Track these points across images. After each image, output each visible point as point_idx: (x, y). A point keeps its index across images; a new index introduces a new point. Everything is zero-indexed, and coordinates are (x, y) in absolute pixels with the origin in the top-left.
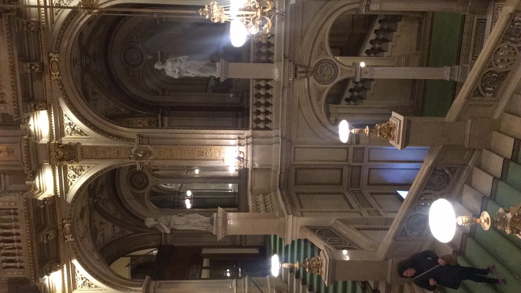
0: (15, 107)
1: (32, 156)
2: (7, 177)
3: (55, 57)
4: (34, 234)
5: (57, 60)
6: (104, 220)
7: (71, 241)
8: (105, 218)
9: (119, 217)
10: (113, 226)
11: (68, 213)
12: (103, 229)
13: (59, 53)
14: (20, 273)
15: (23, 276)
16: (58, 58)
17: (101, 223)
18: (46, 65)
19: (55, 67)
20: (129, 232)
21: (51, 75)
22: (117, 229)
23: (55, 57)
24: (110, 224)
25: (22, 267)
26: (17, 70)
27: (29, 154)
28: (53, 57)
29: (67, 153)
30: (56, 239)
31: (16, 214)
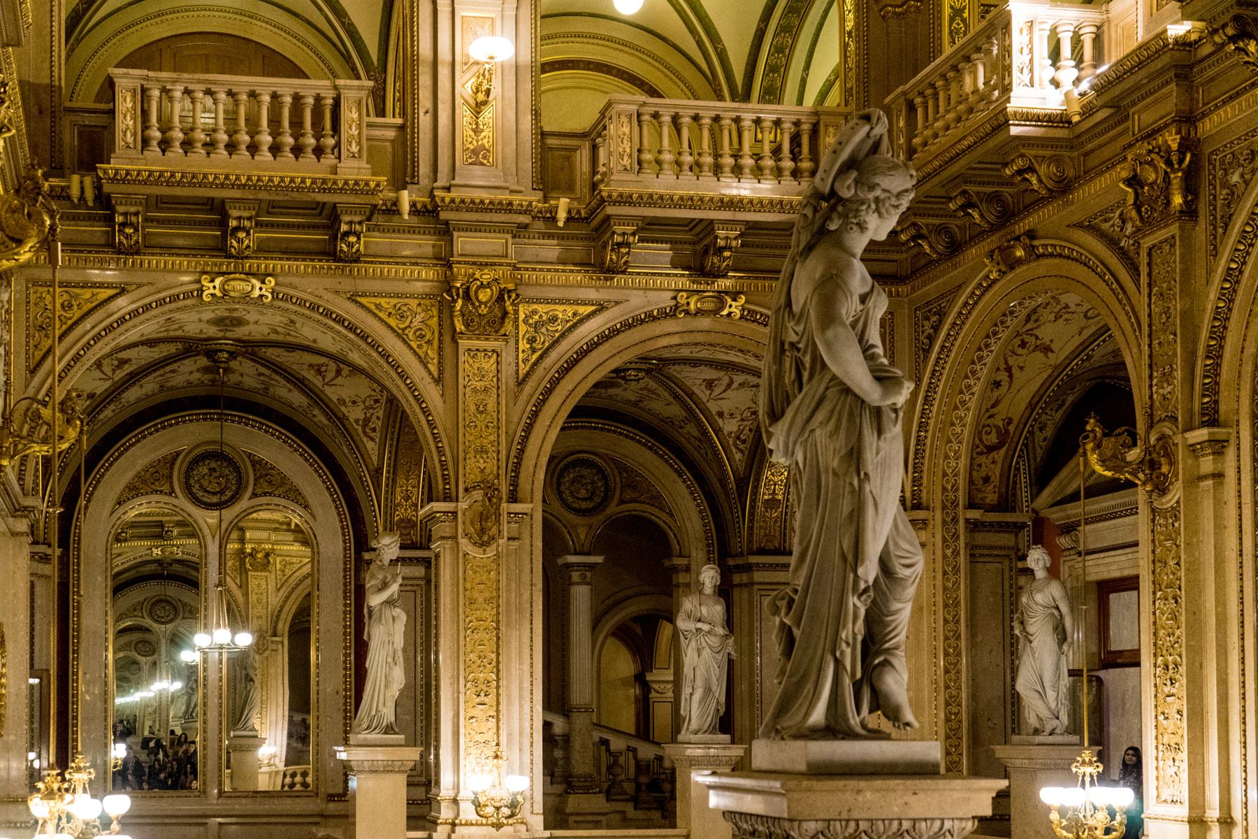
0: (635, 196)
1: (487, 217)
2: (391, 134)
3: (734, 308)
5: (725, 312)
6: (120, 374)
7: (201, 291)
11: (292, 292)
13: (741, 318)
15: (119, 143)
16: (729, 314)
18: (713, 283)
19: (709, 306)
21: (691, 292)
23: (734, 308)
24: (101, 387)
27: (487, 210)
28: (734, 304)
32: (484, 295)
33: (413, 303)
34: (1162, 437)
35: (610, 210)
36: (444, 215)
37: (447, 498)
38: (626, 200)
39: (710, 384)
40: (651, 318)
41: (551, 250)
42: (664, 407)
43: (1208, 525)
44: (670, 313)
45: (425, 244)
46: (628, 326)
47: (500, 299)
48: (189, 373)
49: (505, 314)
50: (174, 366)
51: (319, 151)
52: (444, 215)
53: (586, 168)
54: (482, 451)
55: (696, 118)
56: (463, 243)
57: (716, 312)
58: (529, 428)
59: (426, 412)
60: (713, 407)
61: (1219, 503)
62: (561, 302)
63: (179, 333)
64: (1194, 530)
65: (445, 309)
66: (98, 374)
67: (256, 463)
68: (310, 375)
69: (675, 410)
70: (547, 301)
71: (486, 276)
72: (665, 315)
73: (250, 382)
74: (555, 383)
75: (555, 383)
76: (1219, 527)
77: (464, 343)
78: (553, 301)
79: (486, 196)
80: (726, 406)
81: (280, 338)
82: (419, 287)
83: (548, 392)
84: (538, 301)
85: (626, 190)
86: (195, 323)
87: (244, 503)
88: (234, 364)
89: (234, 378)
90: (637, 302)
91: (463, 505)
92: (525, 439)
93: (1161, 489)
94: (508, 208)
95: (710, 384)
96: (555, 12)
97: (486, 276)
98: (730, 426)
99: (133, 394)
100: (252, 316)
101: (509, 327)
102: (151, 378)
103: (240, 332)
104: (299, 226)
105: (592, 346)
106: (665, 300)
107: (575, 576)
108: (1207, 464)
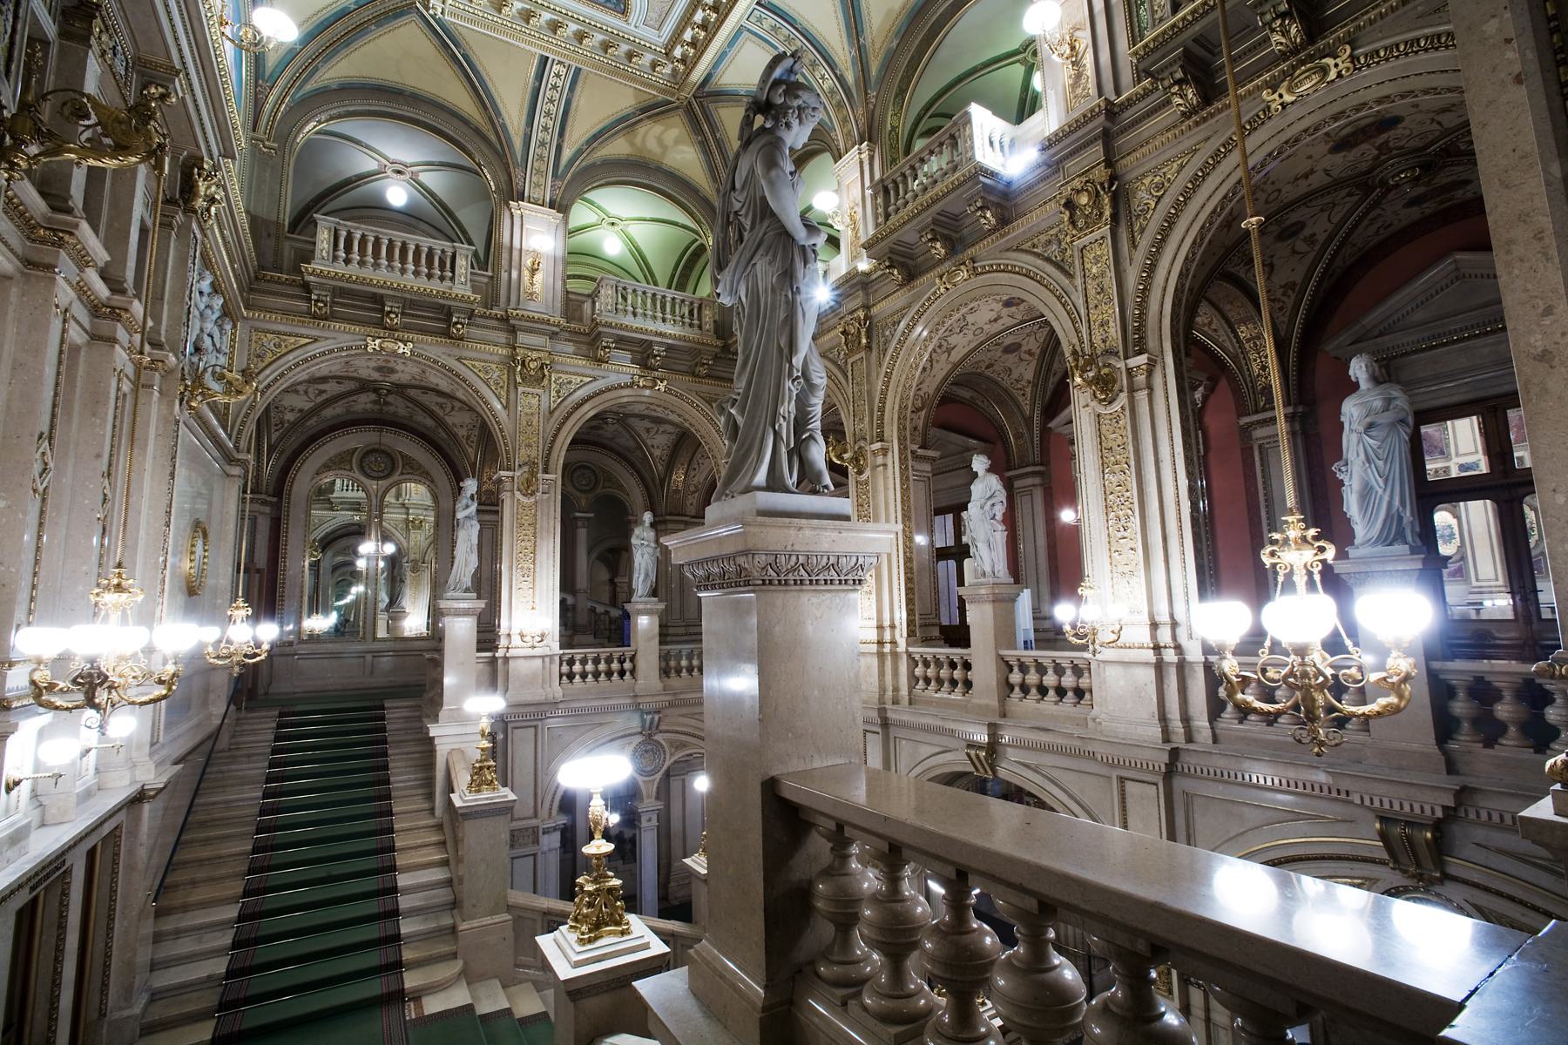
1: (536, 325)
2: (486, 280)
4: (408, 296)
6: (319, 399)
8: (327, 400)
9: (312, 422)
10: (301, 411)
12: (306, 392)
14: (324, 254)
17: (322, 392)
20: (274, 437)
21: (640, 376)
22: (290, 417)
23: (662, 386)
24: (307, 406)
25: (335, 258)
26: (659, 339)
29: (532, 373)
30: (380, 324)
31: (442, 278)
32: (533, 365)
33: (494, 366)
34: (860, 448)
35: (601, 329)
36: (512, 322)
37: (509, 469)
38: (609, 325)
39: (648, 430)
40: (620, 387)
41: (570, 348)
42: (625, 441)
43: (881, 487)
44: (631, 386)
45: (502, 337)
46: (608, 390)
47: (542, 368)
48: (364, 402)
49: (544, 376)
50: (354, 398)
51: (442, 278)
52: (512, 322)
53: (589, 312)
54: (529, 446)
55: (644, 293)
56: (522, 338)
57: (652, 388)
58: (555, 436)
59: (498, 423)
60: (649, 442)
61: (886, 478)
62: (574, 374)
63: (355, 375)
64: (875, 490)
65: (511, 371)
66: (305, 398)
67: (403, 456)
68: (436, 409)
69: (631, 444)
70: (567, 373)
71: (535, 355)
72: (627, 386)
73: (402, 412)
74: (570, 414)
75: (570, 414)
76: (886, 489)
77: (521, 389)
78: (570, 373)
79: (536, 316)
80: (655, 442)
81: (417, 383)
82: (496, 359)
83: (566, 419)
84: (562, 372)
85: (610, 320)
86: (365, 369)
87: (396, 477)
88: (390, 399)
89: (392, 409)
90: (613, 379)
91: (518, 474)
92: (553, 442)
93: (860, 472)
94: (548, 322)
95: (648, 430)
96: (569, 123)
97: (535, 355)
98: (657, 453)
99: (328, 413)
100: (399, 367)
101: (546, 382)
102: (340, 403)
103: (394, 378)
104: (429, 318)
105: (590, 398)
106: (628, 379)
107: (579, 523)
108: (880, 460)
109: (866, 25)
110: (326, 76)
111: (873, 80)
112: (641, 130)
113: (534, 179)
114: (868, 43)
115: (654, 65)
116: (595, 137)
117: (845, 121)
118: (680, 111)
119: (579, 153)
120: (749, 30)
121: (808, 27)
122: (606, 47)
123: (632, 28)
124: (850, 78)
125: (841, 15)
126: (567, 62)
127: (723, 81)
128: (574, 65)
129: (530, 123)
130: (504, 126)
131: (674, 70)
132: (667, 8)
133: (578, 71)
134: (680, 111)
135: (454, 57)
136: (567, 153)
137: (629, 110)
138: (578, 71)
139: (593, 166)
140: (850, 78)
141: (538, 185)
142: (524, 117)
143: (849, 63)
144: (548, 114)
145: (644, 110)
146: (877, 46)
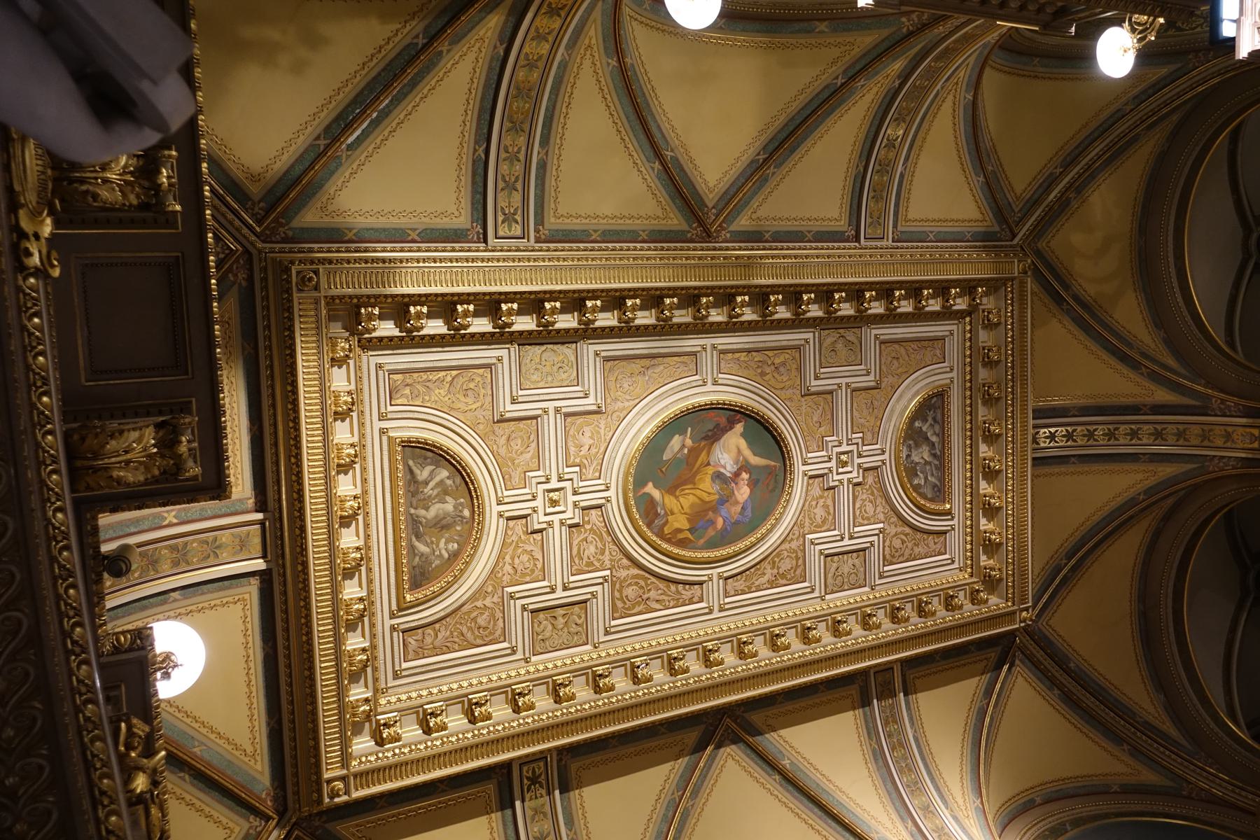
109: (818, 85)
110: (1151, 710)
111: (885, 32)
112: (1090, 290)
113: (1219, 442)
114: (838, 69)
115: (990, 326)
116: (1124, 358)
117: (968, 39)
118: (1042, 245)
119: (1154, 377)
120: (895, 226)
121: (856, 154)
122: (989, 401)
123: (954, 374)
124: (897, 66)
125: (822, 129)
126: (1031, 431)
127: (975, 214)
128: (1031, 422)
129: (1134, 458)
130: (1149, 492)
131: (986, 294)
132: (914, 345)
133: (1039, 413)
134: (1042, 245)
135: (1074, 569)
136: (1163, 396)
137: (1068, 322)
138: (1039, 413)
139: (1171, 343)
140: (897, 66)
141: (1228, 436)
142: (1126, 466)
143: (879, 78)
144: (1111, 435)
145: (1058, 300)
146: (836, 52)
